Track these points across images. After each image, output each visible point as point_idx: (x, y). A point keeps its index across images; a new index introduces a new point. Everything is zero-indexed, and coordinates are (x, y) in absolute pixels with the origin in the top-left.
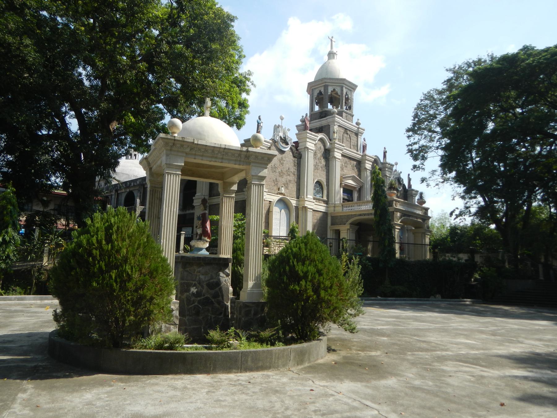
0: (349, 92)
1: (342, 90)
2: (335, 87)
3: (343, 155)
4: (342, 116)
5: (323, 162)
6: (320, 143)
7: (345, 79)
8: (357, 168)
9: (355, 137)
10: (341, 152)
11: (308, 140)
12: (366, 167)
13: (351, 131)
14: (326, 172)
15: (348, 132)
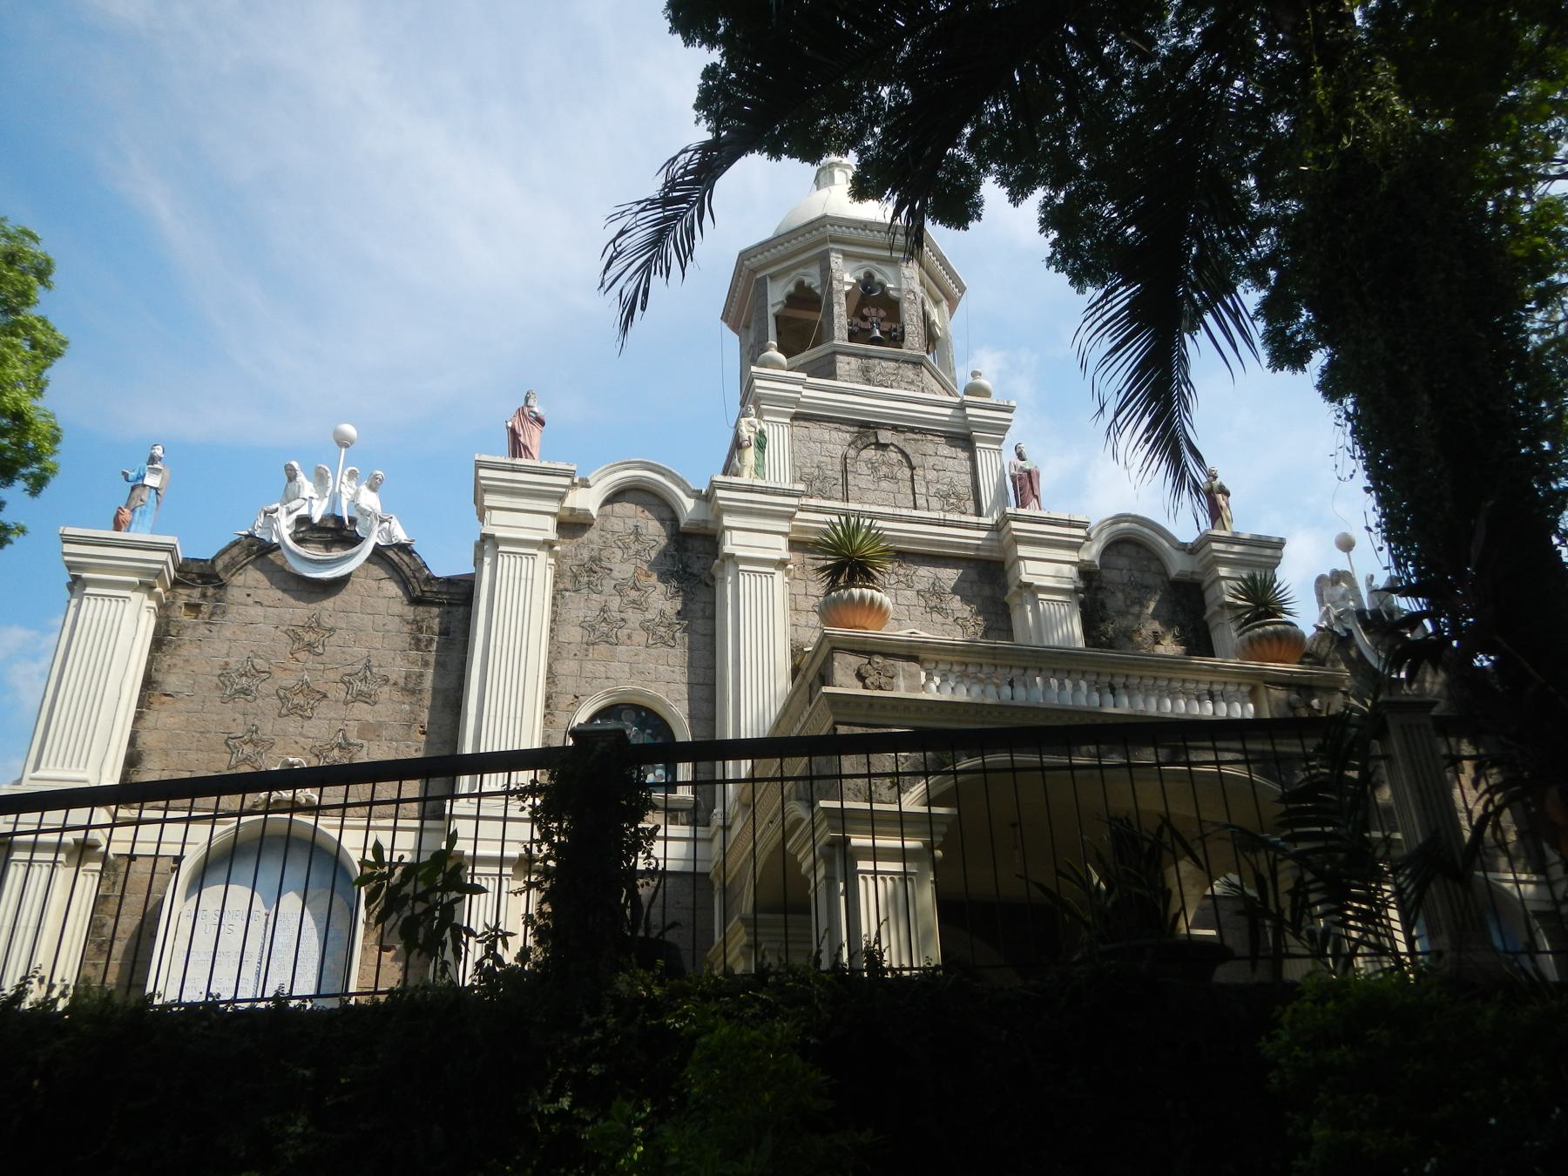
0: (887, 270)
1: (826, 270)
2: (796, 275)
3: (794, 545)
4: (832, 375)
5: (662, 600)
6: (625, 508)
7: (825, 216)
8: (966, 600)
9: (945, 450)
10: (784, 526)
11: (489, 500)
12: (1025, 578)
13: (912, 430)
14: (691, 649)
15: (885, 436)
